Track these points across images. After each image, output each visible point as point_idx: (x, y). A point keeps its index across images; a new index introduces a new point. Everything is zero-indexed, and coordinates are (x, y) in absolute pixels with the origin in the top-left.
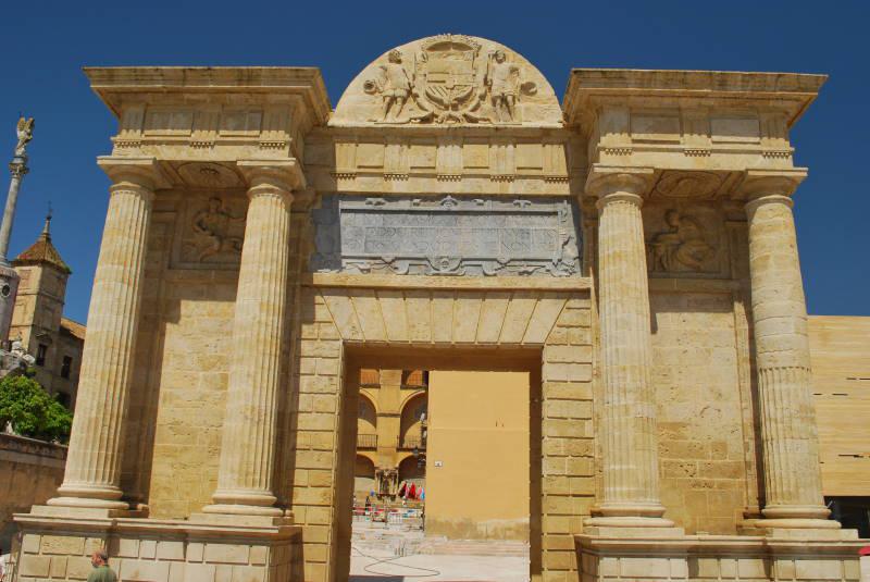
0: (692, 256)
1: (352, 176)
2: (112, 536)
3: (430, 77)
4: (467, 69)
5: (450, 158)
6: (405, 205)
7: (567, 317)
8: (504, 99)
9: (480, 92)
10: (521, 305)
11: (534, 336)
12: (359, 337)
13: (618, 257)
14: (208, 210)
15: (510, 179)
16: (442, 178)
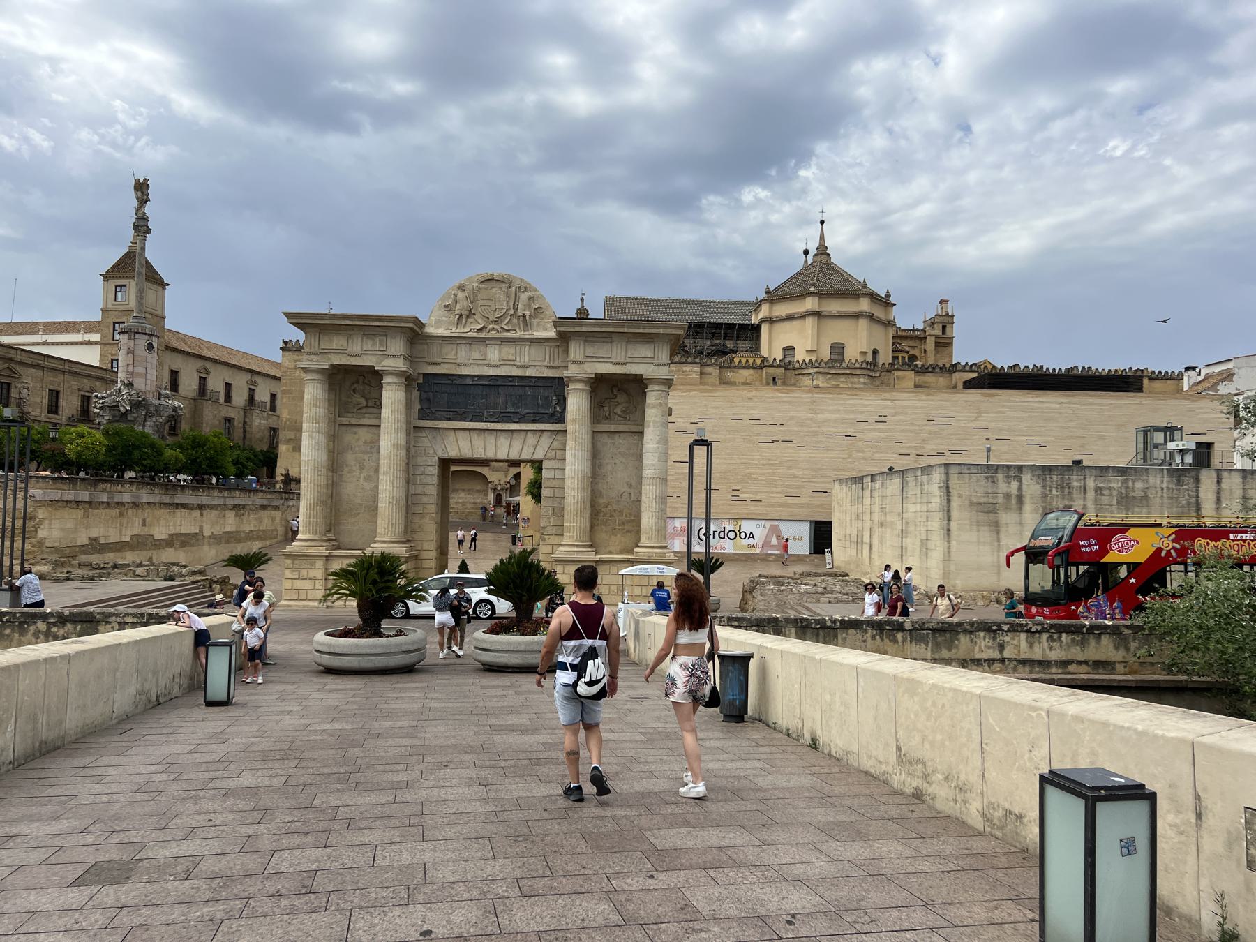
0: (623, 411)
1: (438, 364)
2: (328, 558)
3: (481, 303)
4: (503, 297)
5: (494, 354)
6: (468, 381)
7: (555, 444)
8: (524, 317)
9: (512, 312)
10: (531, 440)
11: (539, 455)
12: (446, 456)
13: (574, 421)
14: (358, 382)
15: (527, 367)
16: (489, 366)
